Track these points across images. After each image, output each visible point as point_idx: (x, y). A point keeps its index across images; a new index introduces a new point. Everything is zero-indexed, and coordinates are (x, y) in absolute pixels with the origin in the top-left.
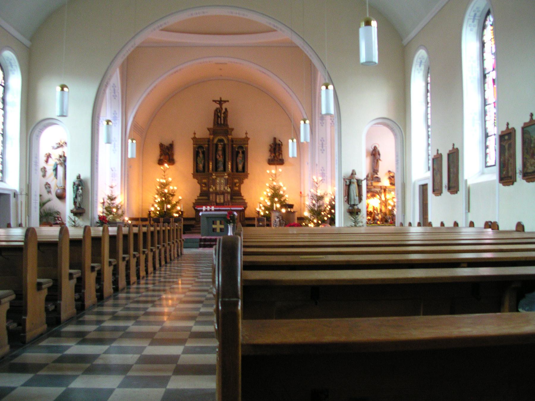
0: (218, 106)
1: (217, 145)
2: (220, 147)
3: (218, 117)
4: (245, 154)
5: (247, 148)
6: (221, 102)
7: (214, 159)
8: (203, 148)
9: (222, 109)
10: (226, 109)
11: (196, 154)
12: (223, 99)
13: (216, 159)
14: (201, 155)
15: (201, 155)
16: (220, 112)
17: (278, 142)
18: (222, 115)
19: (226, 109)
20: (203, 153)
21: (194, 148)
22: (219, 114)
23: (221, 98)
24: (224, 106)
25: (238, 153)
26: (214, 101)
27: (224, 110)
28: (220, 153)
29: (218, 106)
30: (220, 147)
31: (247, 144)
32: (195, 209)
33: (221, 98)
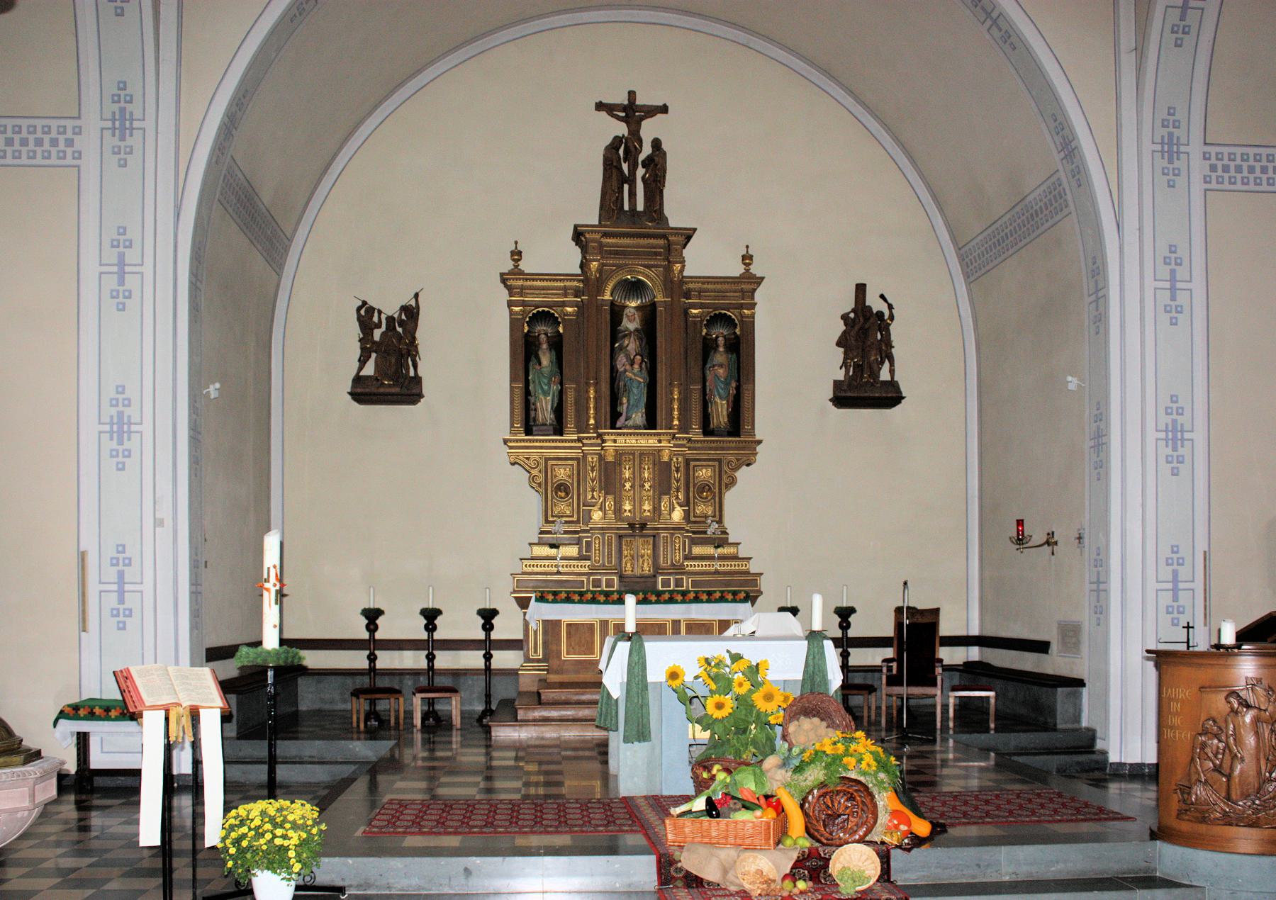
0: (622, 129)
1: (616, 313)
2: (631, 324)
3: (623, 180)
4: (742, 349)
5: (749, 326)
6: (632, 113)
7: (605, 374)
8: (556, 322)
9: (640, 141)
10: (656, 144)
11: (525, 351)
12: (640, 101)
13: (614, 374)
14: (546, 359)
15: (546, 359)
16: (631, 155)
17: (876, 304)
18: (640, 172)
19: (656, 144)
20: (557, 344)
21: (514, 324)
22: (625, 167)
23: (632, 94)
24: (649, 129)
25: (708, 347)
26: (600, 106)
27: (647, 150)
28: (632, 345)
29: (622, 129)
30: (631, 324)
31: (753, 306)
32: (506, 286)
33: (632, 94)
